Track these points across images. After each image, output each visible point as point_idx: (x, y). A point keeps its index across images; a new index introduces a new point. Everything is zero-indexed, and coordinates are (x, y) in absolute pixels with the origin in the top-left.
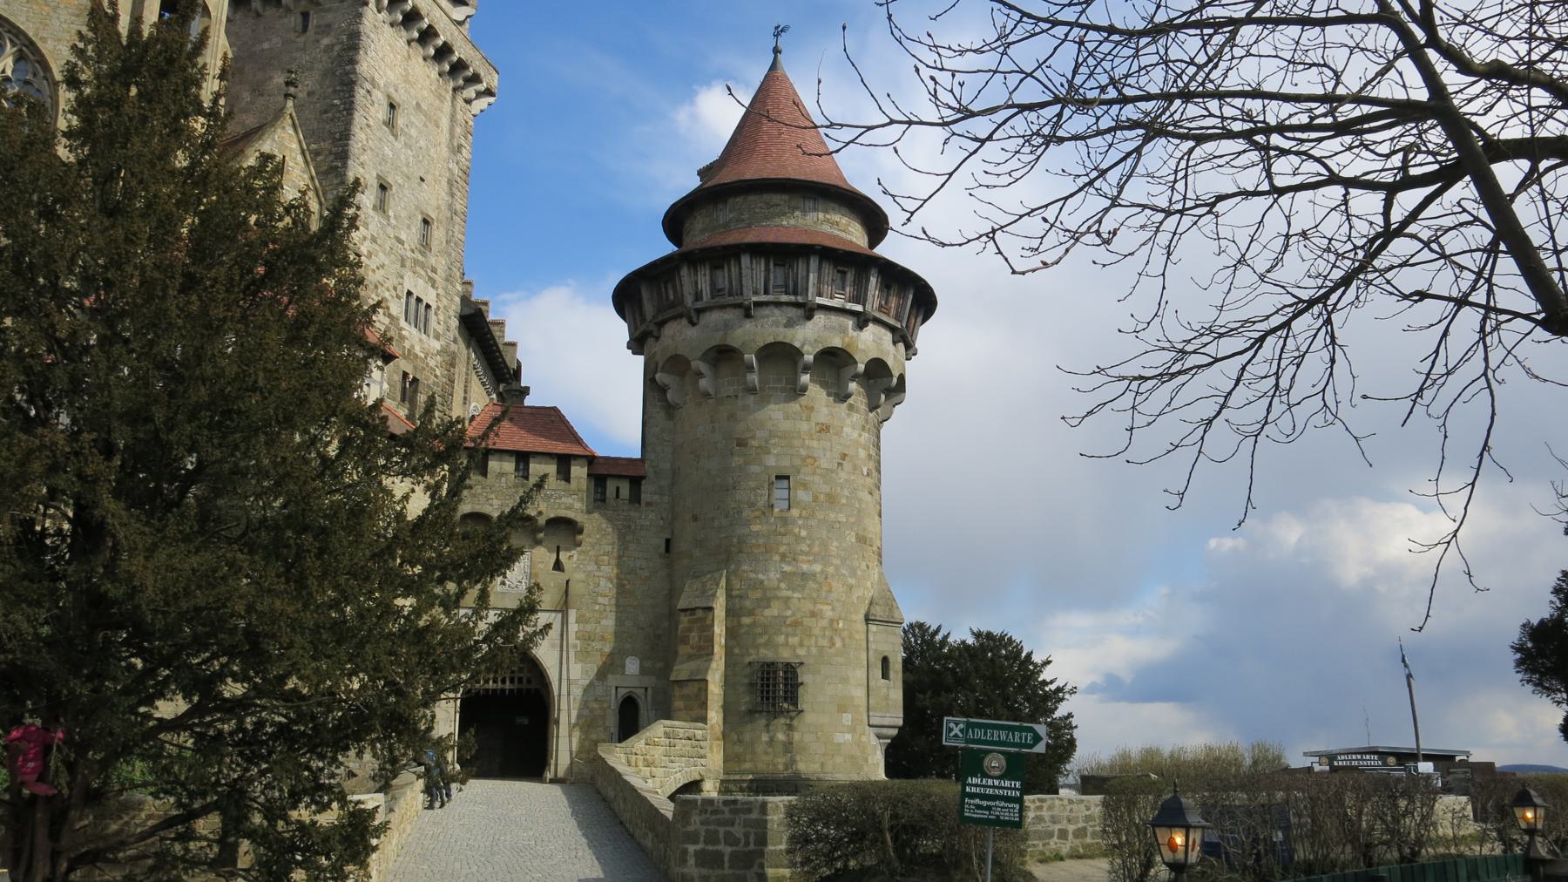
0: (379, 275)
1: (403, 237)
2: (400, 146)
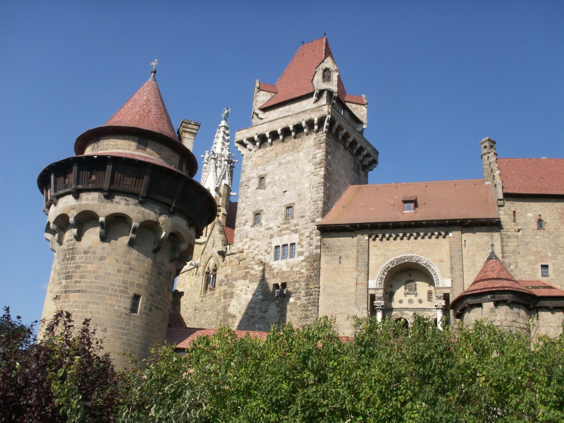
0: (255, 252)
1: (272, 225)
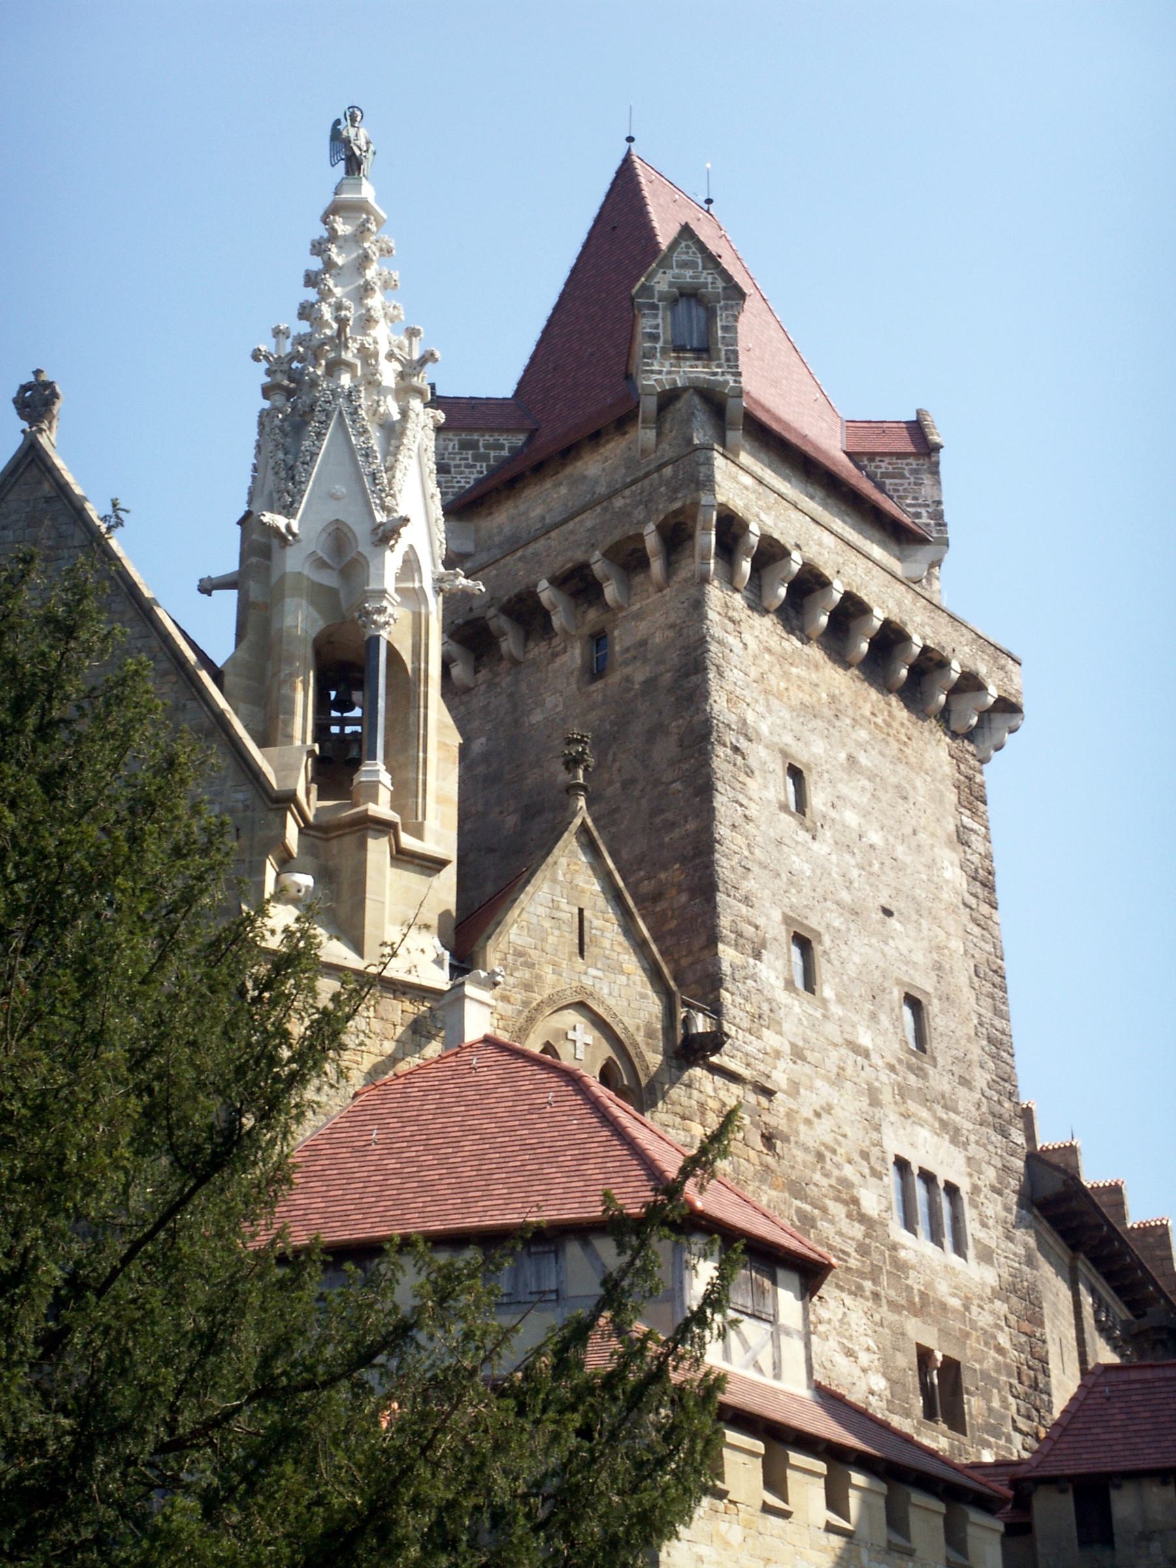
0: (822, 1131)
1: (865, 1039)
2: (825, 850)
